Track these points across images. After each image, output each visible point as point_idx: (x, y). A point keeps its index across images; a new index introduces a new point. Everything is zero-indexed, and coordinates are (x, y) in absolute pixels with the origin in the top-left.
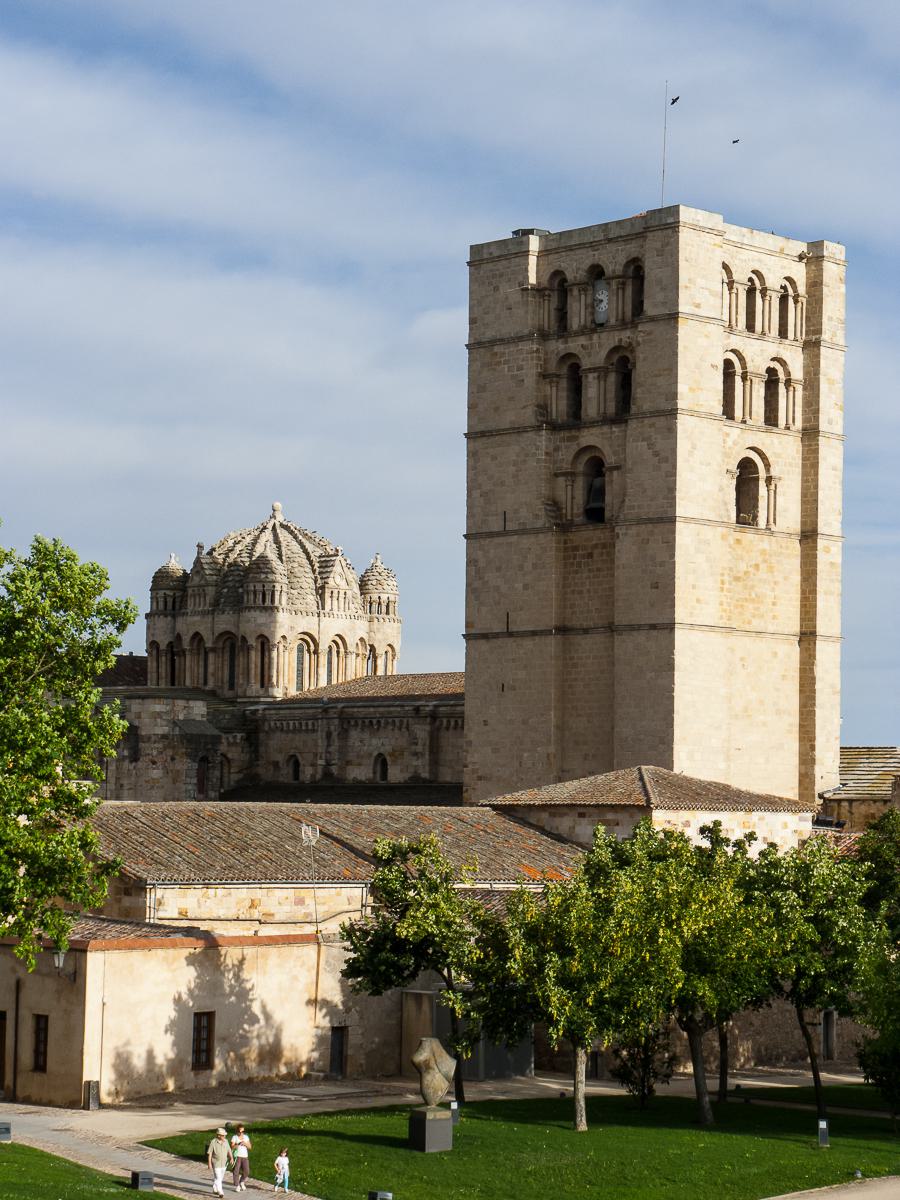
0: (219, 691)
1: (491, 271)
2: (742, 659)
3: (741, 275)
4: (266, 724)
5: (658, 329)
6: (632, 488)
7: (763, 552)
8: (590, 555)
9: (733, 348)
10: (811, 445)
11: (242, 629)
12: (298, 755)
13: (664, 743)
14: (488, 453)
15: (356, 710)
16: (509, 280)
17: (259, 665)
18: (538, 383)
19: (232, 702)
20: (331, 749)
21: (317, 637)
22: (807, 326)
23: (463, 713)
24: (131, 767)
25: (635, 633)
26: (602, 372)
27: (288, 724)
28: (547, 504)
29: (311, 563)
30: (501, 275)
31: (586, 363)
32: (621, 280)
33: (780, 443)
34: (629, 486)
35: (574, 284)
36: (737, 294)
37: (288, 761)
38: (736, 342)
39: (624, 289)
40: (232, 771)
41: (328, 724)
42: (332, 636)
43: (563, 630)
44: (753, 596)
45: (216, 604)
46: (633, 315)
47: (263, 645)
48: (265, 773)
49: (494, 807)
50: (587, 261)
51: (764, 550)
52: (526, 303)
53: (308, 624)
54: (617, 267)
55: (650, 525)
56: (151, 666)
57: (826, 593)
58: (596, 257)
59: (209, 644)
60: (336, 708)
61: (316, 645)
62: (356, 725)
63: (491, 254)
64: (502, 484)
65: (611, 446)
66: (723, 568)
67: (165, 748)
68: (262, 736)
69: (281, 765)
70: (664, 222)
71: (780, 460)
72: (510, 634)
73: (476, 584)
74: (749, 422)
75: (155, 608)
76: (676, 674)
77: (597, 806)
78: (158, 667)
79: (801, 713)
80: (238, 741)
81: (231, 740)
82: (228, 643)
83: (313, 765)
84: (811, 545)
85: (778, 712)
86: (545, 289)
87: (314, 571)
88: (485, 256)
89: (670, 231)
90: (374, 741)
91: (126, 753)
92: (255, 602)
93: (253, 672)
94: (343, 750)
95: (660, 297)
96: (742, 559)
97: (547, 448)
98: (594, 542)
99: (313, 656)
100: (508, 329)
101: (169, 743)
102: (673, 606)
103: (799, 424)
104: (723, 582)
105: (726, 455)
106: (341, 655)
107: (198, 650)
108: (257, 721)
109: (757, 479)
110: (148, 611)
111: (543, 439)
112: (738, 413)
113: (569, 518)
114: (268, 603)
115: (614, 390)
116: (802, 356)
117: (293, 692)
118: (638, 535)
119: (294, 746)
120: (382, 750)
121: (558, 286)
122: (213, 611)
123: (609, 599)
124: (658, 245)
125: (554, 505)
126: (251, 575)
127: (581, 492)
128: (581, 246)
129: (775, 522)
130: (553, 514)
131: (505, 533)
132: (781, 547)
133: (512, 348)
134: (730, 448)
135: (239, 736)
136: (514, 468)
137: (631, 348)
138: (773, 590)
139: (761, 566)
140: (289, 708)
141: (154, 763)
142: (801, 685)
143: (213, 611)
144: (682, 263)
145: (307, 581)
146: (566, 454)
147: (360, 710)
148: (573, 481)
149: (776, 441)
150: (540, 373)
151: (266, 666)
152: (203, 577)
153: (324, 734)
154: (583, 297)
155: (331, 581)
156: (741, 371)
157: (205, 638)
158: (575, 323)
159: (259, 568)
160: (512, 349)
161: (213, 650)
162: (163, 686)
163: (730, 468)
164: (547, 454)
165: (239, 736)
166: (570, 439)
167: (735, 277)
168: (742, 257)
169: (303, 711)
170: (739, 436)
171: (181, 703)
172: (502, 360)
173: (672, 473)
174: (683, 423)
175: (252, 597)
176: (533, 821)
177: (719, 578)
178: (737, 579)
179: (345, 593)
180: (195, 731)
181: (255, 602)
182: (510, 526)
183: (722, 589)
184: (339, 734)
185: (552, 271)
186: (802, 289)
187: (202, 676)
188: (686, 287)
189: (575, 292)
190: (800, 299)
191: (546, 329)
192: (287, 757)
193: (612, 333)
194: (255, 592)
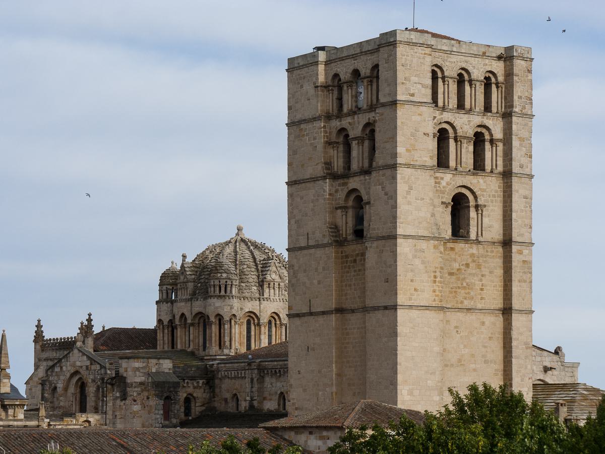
0: (196, 352)
1: (299, 75)
2: (456, 327)
3: (451, 70)
4: (220, 373)
5: (386, 111)
6: (374, 216)
7: (472, 255)
8: (355, 261)
9: (446, 120)
10: (508, 183)
11: (207, 310)
12: (238, 394)
13: (392, 385)
14: (298, 195)
15: (267, 363)
16: (309, 81)
17: (218, 334)
18: (325, 148)
19: (202, 359)
20: (254, 389)
21: (258, 315)
22: (505, 103)
23: (288, 364)
24: (122, 404)
25: (376, 312)
26: (361, 140)
27: (231, 373)
28: (330, 228)
29: (256, 265)
30: (304, 78)
31: (352, 134)
32: (369, 79)
33: (485, 182)
34: (372, 215)
35: (344, 83)
36: (448, 85)
37: (233, 398)
38: (447, 116)
39: (371, 85)
40: (197, 405)
41: (252, 373)
42: (269, 313)
43: (340, 311)
44: (465, 284)
45: (194, 294)
47: (220, 320)
48: (220, 406)
49: (266, 428)
50: (351, 67)
51: (473, 254)
52: (317, 96)
53: (250, 306)
54: (367, 71)
55: (384, 241)
56: (159, 336)
57: (519, 281)
58: (356, 64)
59: (189, 321)
60: (255, 362)
61: (259, 319)
62: (268, 374)
63: (299, 64)
66: (436, 268)
67: (142, 391)
68: (217, 381)
69: (228, 400)
70: (388, 41)
71: (485, 193)
72: (311, 314)
74: (460, 169)
75: (161, 298)
76: (399, 339)
77: (317, 427)
78: (163, 337)
79: (504, 362)
80: (200, 385)
81: (195, 384)
82: (202, 321)
83: (245, 400)
84: (508, 249)
85: (486, 362)
86: (329, 86)
87: (258, 270)
88: (296, 65)
89: (392, 47)
90: (279, 384)
91: (118, 394)
92: (214, 292)
93: (213, 339)
94: (261, 391)
95: (387, 90)
96: (455, 260)
97: (330, 190)
98: (357, 252)
99: (257, 328)
100: (308, 114)
101: (145, 388)
102: (396, 294)
103: (500, 168)
104: (435, 277)
105: (440, 192)
106: (278, 326)
107: (185, 324)
108: (214, 371)
109: (469, 207)
110: (158, 299)
111: (327, 185)
112: (452, 163)
113: (344, 236)
114: (223, 293)
115: (367, 151)
116: (502, 123)
117: (243, 350)
118: (377, 247)
119: (235, 388)
120: (282, 390)
121: (336, 85)
122: (191, 299)
123: (364, 291)
124: (386, 56)
125: (335, 228)
126: (212, 275)
127: (351, 219)
128: (348, 57)
129: (482, 235)
130: (334, 234)
131: (308, 247)
132: (487, 251)
133: (310, 126)
134: (443, 187)
135: (201, 382)
136: (312, 204)
137: (375, 121)
138: (481, 280)
139: (471, 265)
140: (232, 363)
141: (135, 401)
142: (504, 343)
143: (191, 299)
144: (399, 68)
145: (252, 277)
146: (341, 195)
147: (270, 363)
148: (346, 212)
149: (481, 181)
150: (327, 141)
151: (222, 335)
152: (185, 277)
153: (249, 379)
154: (350, 90)
155: (268, 278)
156: (454, 135)
157: (187, 317)
158: (345, 110)
159: (217, 270)
160: (310, 126)
161: (192, 324)
162: (166, 349)
163: (444, 200)
164: (330, 194)
165: (201, 382)
166: (345, 184)
167: (446, 74)
168: (453, 60)
169: (239, 364)
170: (451, 178)
171: (154, 361)
172: (305, 133)
173: (395, 206)
174: (402, 174)
175: (212, 289)
176: (287, 437)
177: (433, 274)
178: (451, 274)
179: (279, 284)
180: (162, 379)
181: (214, 292)
182: (311, 243)
183: (435, 282)
184: (257, 380)
185: (333, 74)
186: (501, 79)
187: (187, 342)
188: (402, 83)
189: (345, 88)
190: (499, 85)
191: (331, 112)
192: (231, 396)
193: (365, 114)
194: (214, 286)
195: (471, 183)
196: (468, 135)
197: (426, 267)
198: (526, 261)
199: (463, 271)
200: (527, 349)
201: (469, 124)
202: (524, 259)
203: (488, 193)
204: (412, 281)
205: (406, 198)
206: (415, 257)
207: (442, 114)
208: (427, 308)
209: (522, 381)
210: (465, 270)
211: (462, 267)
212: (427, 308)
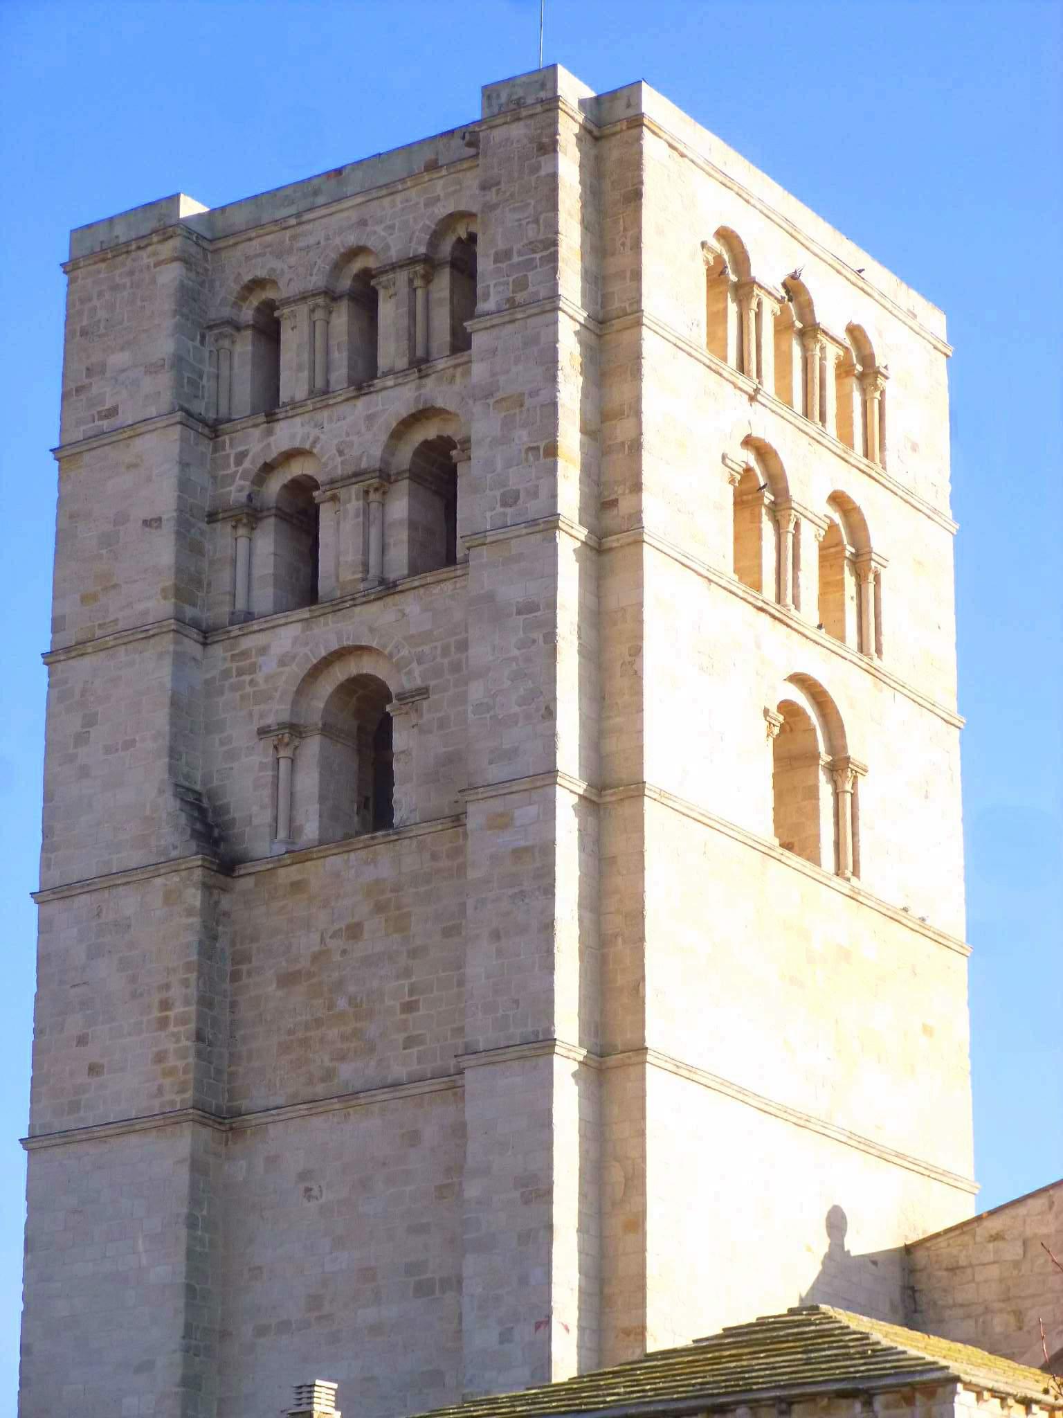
2: (304, 1175)
44: (342, 1003)
57: (496, 935)
71: (426, 649)
104: (165, 1005)
134: (268, 679)
139: (367, 926)
163: (270, 720)
170: (295, 640)
177: (156, 998)
195: (372, 630)
196: (364, 465)
197: (133, 979)
198: (526, 849)
199: (337, 958)
200: (527, 1202)
201: (368, 429)
202: (522, 843)
203: (438, 644)
204: (82, 1040)
205: (71, 759)
206: (95, 952)
207: (270, 433)
208: (127, 1126)
209: (501, 1342)
210: (344, 952)
211: (335, 944)
212: (127, 1126)
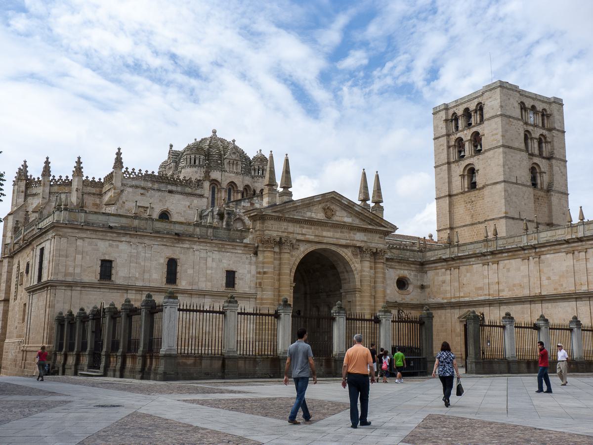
8: (538, 199)
46: (480, 121)
64: (515, 166)
65: (542, 165)
73: (508, 199)
118: (558, 196)
131: (516, 183)
133: (516, 121)
173: (566, 180)
